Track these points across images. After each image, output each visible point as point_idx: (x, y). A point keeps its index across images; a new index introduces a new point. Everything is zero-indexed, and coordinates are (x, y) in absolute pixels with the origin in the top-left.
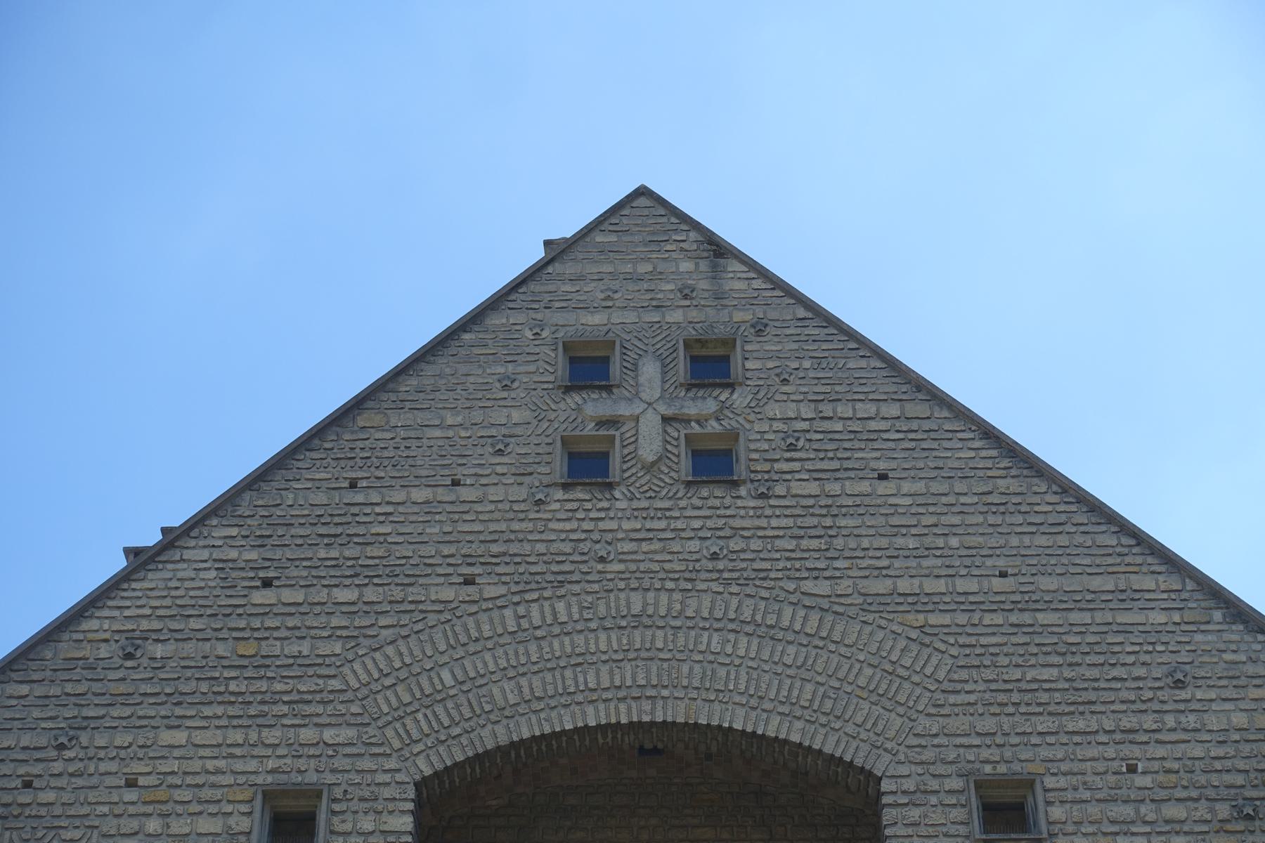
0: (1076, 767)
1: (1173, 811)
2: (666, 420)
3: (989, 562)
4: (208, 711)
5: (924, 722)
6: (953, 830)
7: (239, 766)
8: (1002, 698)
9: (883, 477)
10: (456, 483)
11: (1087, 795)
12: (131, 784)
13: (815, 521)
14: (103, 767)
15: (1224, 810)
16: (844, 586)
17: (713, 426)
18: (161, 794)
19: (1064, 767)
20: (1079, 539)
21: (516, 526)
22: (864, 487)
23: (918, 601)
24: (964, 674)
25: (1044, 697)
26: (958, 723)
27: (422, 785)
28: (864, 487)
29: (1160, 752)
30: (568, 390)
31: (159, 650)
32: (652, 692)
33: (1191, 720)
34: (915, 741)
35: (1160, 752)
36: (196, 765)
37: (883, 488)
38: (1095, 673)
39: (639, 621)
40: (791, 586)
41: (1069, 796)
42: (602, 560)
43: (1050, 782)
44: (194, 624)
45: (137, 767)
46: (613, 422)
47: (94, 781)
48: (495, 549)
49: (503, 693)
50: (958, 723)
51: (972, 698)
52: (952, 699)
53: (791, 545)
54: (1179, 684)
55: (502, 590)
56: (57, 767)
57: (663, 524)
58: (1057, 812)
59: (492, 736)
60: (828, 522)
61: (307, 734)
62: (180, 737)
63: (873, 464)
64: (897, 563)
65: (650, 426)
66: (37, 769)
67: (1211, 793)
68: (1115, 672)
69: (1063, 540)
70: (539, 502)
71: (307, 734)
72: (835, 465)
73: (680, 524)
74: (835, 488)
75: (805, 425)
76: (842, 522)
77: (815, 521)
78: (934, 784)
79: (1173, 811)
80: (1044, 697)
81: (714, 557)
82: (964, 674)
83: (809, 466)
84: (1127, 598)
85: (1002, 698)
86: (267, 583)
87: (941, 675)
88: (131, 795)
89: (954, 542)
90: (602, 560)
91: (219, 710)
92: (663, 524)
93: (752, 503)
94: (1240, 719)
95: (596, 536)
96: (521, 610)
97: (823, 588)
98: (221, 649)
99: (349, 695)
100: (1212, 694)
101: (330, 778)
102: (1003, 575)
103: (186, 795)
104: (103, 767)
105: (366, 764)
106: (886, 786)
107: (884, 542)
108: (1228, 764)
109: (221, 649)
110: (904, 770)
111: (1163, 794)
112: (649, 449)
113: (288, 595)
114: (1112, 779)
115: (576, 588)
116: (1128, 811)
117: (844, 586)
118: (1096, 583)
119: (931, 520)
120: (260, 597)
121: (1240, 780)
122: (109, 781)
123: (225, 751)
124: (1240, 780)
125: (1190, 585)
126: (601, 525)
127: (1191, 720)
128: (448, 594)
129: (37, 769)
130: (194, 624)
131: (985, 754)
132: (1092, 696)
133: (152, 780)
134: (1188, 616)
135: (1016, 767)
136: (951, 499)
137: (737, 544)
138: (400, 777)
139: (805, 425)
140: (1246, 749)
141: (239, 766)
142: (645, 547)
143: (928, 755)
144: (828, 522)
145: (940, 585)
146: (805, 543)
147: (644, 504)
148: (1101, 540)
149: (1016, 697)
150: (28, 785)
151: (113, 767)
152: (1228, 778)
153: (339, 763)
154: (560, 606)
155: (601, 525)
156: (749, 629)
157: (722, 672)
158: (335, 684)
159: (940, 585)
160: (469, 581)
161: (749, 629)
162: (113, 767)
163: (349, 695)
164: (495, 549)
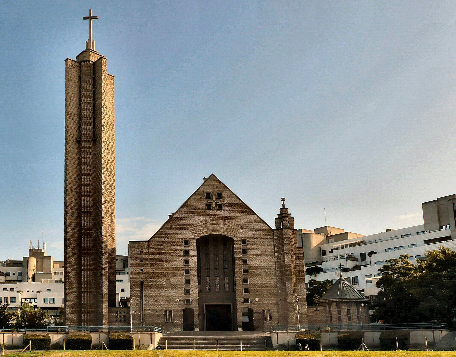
0: (250, 238)
1: (257, 242)
2: (215, 202)
3: (244, 218)
4: (178, 233)
5: (237, 234)
6: (239, 244)
7: (182, 238)
8: (244, 232)
9: (235, 208)
10: (197, 209)
11: (250, 241)
12: (173, 239)
13: (229, 213)
14: (171, 238)
15: (261, 242)
16: (231, 220)
17: (220, 203)
18: (175, 240)
19: (249, 238)
20: (252, 215)
21: (203, 214)
22: (233, 210)
23: (238, 222)
24: (241, 229)
25: (247, 231)
26: (240, 234)
27: (197, 240)
28: (233, 210)
29: (257, 237)
30: (206, 199)
31: (173, 227)
32: (215, 231)
33: (260, 234)
34: (237, 236)
35: (257, 237)
36: (178, 238)
37: (235, 210)
38: (252, 229)
39: (214, 224)
40: (227, 220)
41: (249, 241)
42: (210, 218)
43: (248, 240)
44: (176, 224)
45: (173, 238)
46: (211, 203)
47: (170, 239)
48: (201, 216)
49: (203, 231)
50: (240, 234)
51: (242, 232)
52: (240, 232)
53: (227, 216)
54: (259, 230)
55: (202, 221)
56: (167, 238)
57: (215, 214)
58: (248, 242)
59: (202, 235)
60: (230, 213)
61: (187, 235)
62: (176, 235)
63: (234, 207)
64: (236, 218)
65: (214, 203)
66: (165, 238)
67: (260, 240)
68: (254, 229)
69: (250, 215)
70: (205, 212)
71: (187, 235)
72: (231, 207)
73: (217, 214)
74: (230, 210)
75: (228, 203)
76: (231, 213)
77: (229, 213)
78: (238, 240)
79: (257, 242)
80: (247, 231)
81: (220, 217)
82: (241, 229)
83: (228, 207)
84: (255, 221)
85: (244, 232)
86: (182, 220)
87: (239, 229)
88: (173, 241)
89: (241, 216)
90: (210, 218)
91: (179, 233)
92: (215, 214)
93: (223, 211)
94: (264, 234)
95: (210, 215)
96: (204, 223)
97: (229, 220)
98: (179, 227)
99: (190, 231)
100: (262, 231)
101: (189, 239)
102: (245, 219)
103: (177, 241)
104: (171, 238)
105: (192, 238)
106: (234, 240)
107: (234, 216)
108: (262, 238)
109: (179, 227)
110: (236, 238)
111: (257, 241)
112: (214, 206)
113: (184, 221)
114: (253, 239)
115: (208, 221)
116: (253, 242)
117: (231, 220)
118: (253, 220)
119: (239, 213)
120: (182, 221)
121: (263, 239)
122: (171, 239)
123: (180, 237)
124: (263, 239)
125: (261, 220)
126: (210, 214)
127: (260, 234)
128: (197, 221)
129: (165, 238)
130: (176, 224)
131: (242, 237)
132: (251, 231)
133: (175, 239)
134: (261, 223)
135: (245, 238)
136: (241, 211)
137: (222, 216)
138: (195, 239)
139: (228, 203)
140: (264, 236)
141: (182, 238)
142: (214, 216)
143: (238, 237)
144: (230, 213)
145: (239, 220)
146: (228, 216)
147: (214, 212)
148: (254, 215)
149: (245, 231)
150: (165, 240)
151: (171, 238)
152: (262, 239)
153: (190, 238)
154: (207, 222)
155: (210, 214)
156: (223, 225)
157: (221, 229)
158: (189, 230)
159: (239, 220)
160: (199, 220)
161: (223, 225)
162: (171, 238)
163: (190, 231)
164: (201, 216)
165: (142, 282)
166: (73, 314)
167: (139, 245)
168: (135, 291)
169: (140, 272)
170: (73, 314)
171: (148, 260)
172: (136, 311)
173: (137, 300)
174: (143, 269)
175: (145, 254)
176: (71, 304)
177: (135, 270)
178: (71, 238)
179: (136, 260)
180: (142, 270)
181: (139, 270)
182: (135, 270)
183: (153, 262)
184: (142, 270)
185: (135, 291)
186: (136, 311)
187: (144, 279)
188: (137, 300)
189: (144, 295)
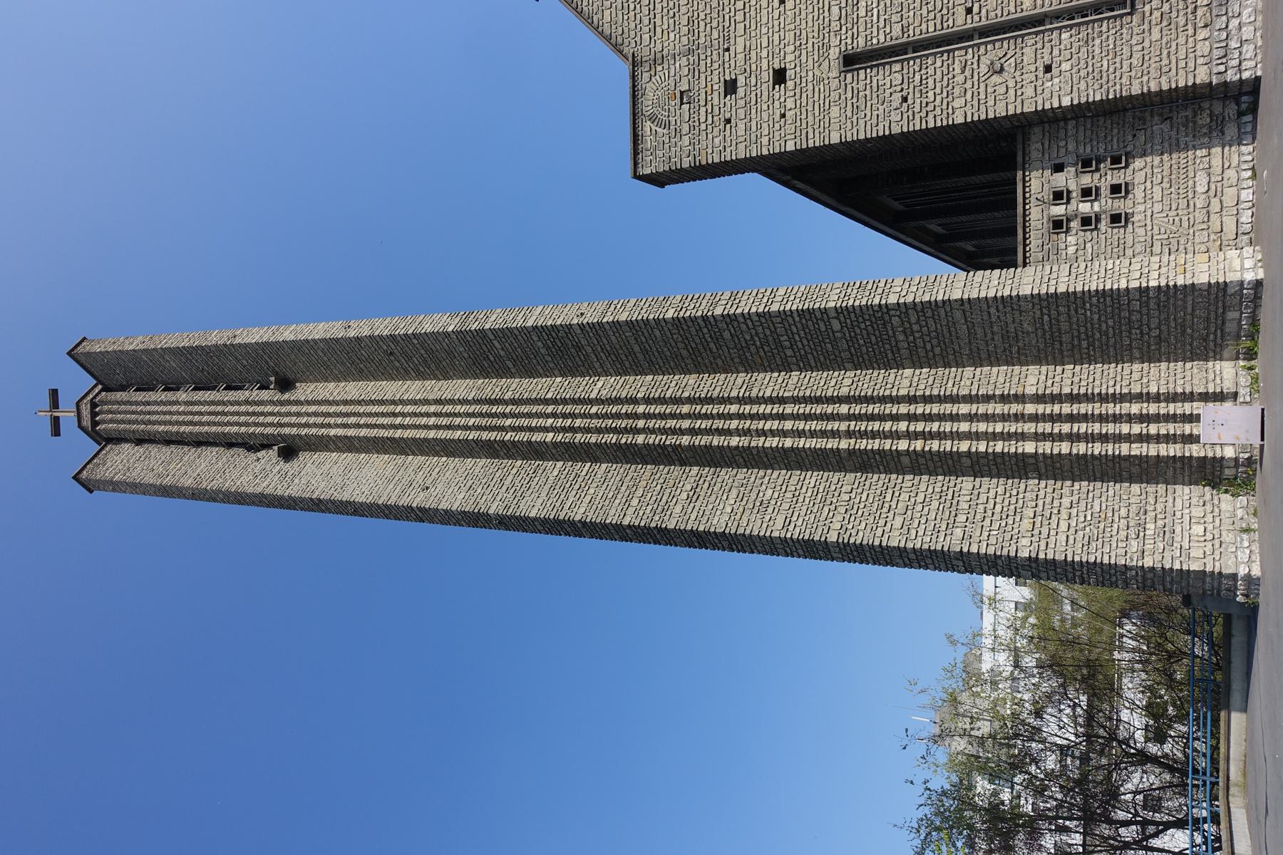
165: (851, 61)
166: (1064, 515)
167: (653, 118)
168: (905, 99)
169: (790, 84)
170: (1064, 515)
171: (728, 50)
172: (1048, 69)
173: (968, 73)
174: (777, 66)
175: (693, 71)
176: (987, 522)
177: (777, 117)
178: (617, 501)
179: (728, 121)
180: (780, 76)
181: (779, 91)
182: (783, 116)
183: (739, 17)
184: (780, 76)
185: (905, 99)
186: (1048, 69)
187: (834, 53)
188: (968, 73)
189: (930, 29)
